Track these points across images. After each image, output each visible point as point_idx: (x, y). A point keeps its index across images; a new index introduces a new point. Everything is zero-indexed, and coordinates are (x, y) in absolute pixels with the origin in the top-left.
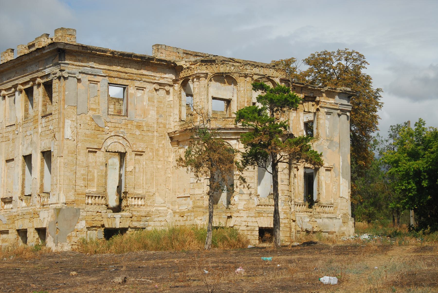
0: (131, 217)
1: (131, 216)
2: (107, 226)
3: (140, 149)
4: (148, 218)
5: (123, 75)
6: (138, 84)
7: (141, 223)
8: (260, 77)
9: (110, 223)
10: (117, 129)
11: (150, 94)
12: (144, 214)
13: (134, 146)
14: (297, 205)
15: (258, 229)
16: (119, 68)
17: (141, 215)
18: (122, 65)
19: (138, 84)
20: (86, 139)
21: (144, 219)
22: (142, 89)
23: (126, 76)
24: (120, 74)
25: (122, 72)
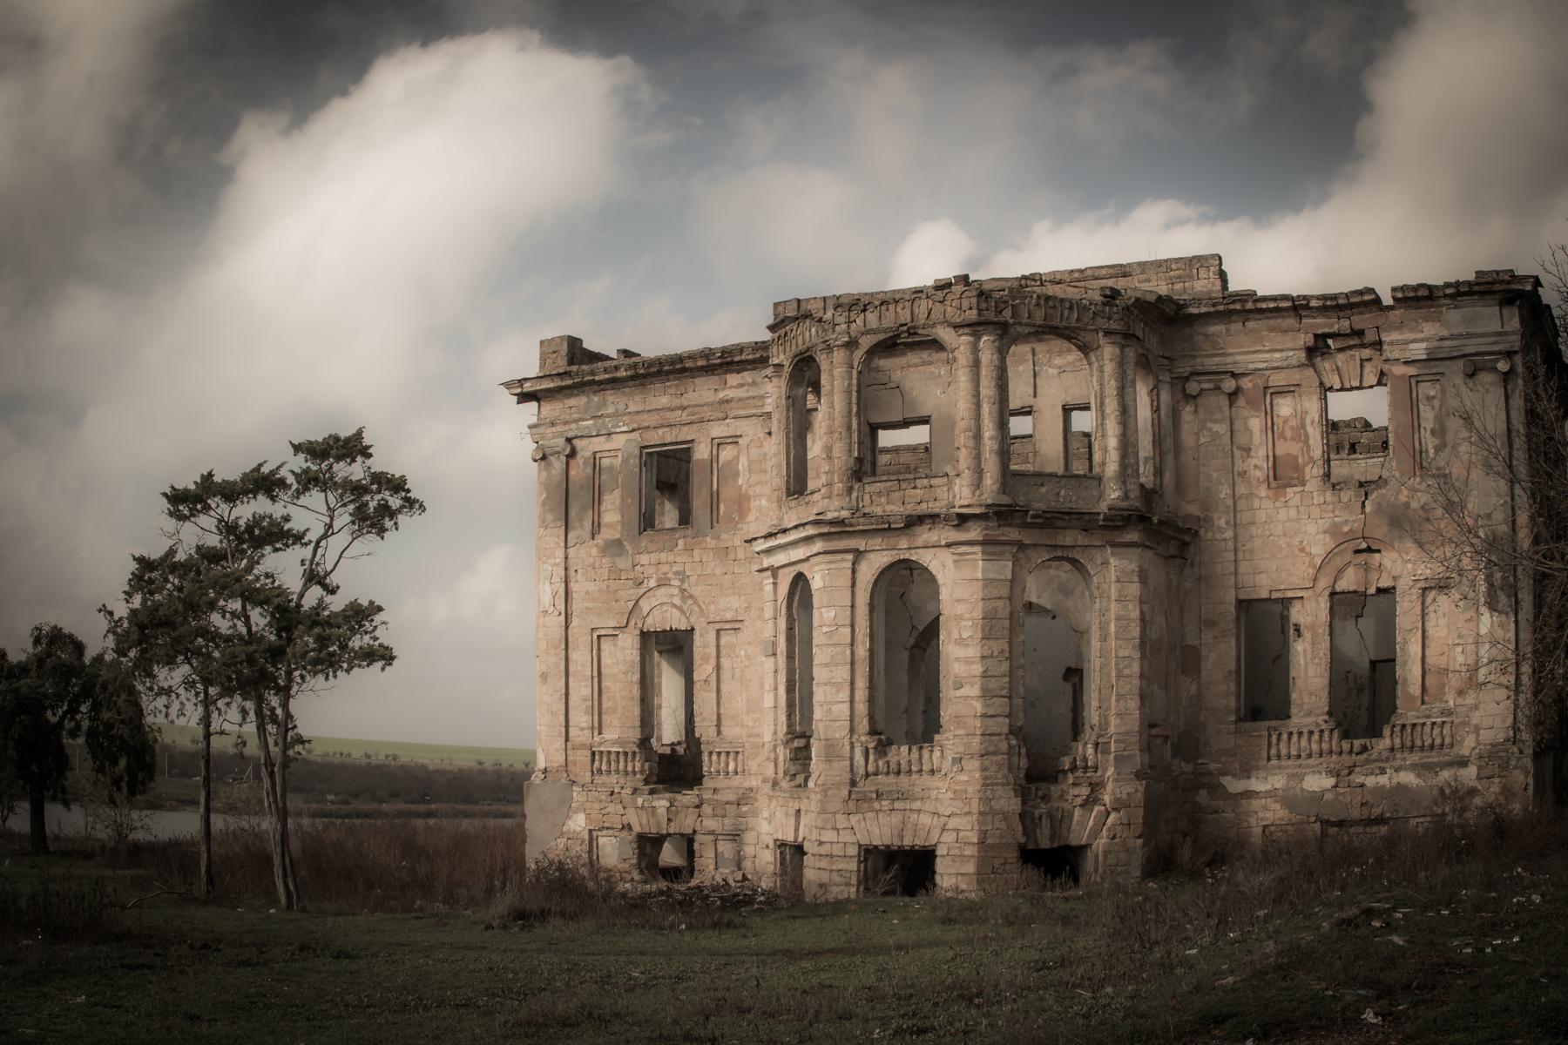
0: (698, 807)
1: (697, 801)
2: (637, 829)
3: (729, 616)
4: (744, 809)
5: (676, 416)
6: (718, 430)
7: (727, 821)
8: (881, 337)
9: (644, 822)
10: (665, 568)
11: (754, 452)
12: (731, 797)
13: (712, 608)
14: (1300, 734)
15: (853, 851)
16: (664, 400)
17: (725, 799)
18: (672, 391)
19: (718, 430)
20: (590, 605)
21: (731, 809)
22: (734, 440)
23: (685, 417)
24: (668, 414)
25: (672, 410)
